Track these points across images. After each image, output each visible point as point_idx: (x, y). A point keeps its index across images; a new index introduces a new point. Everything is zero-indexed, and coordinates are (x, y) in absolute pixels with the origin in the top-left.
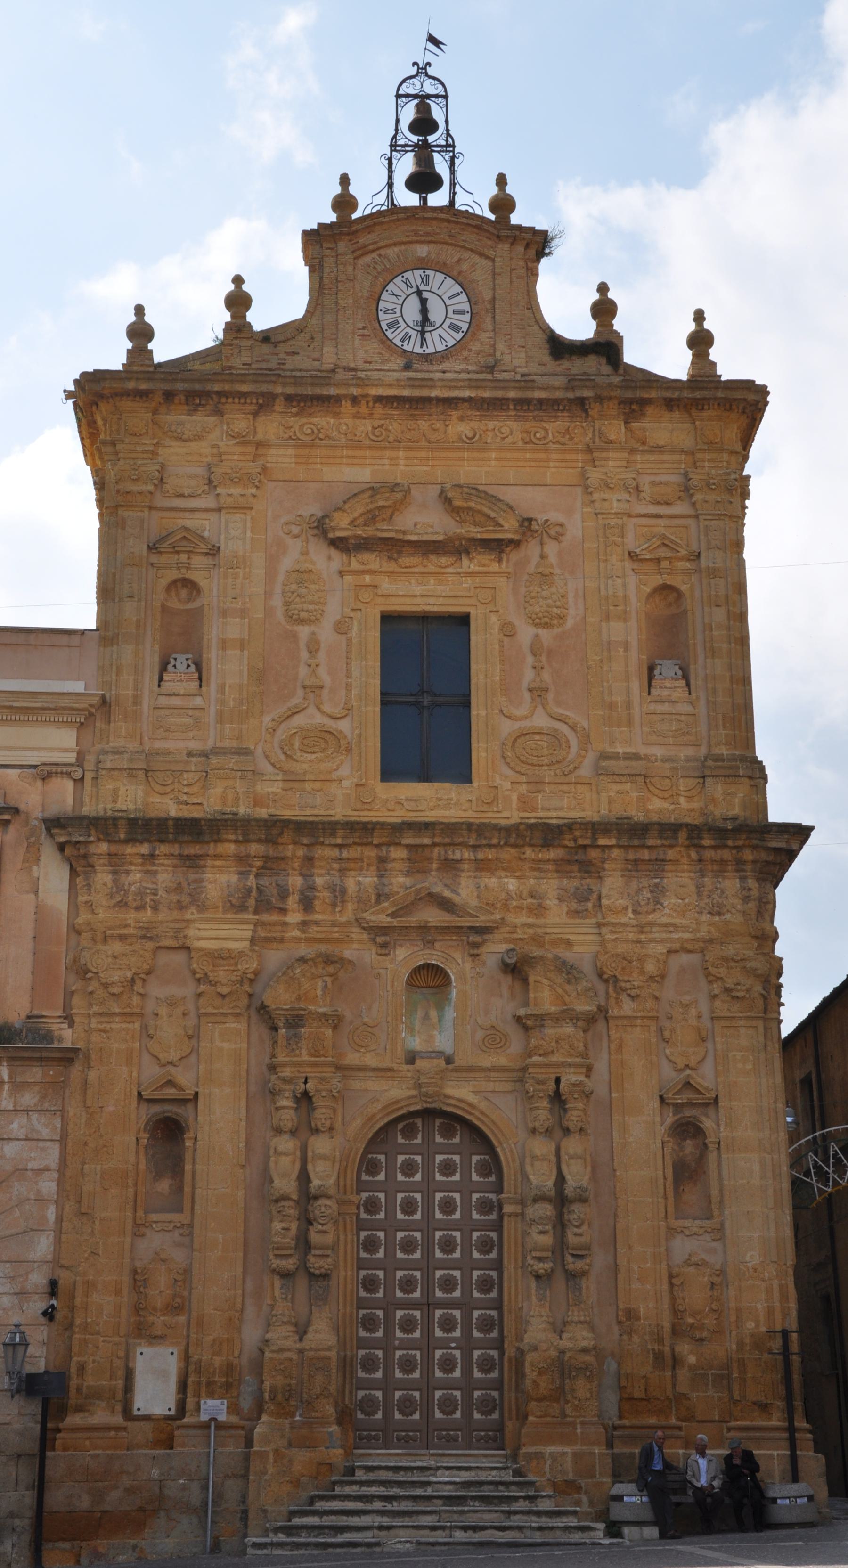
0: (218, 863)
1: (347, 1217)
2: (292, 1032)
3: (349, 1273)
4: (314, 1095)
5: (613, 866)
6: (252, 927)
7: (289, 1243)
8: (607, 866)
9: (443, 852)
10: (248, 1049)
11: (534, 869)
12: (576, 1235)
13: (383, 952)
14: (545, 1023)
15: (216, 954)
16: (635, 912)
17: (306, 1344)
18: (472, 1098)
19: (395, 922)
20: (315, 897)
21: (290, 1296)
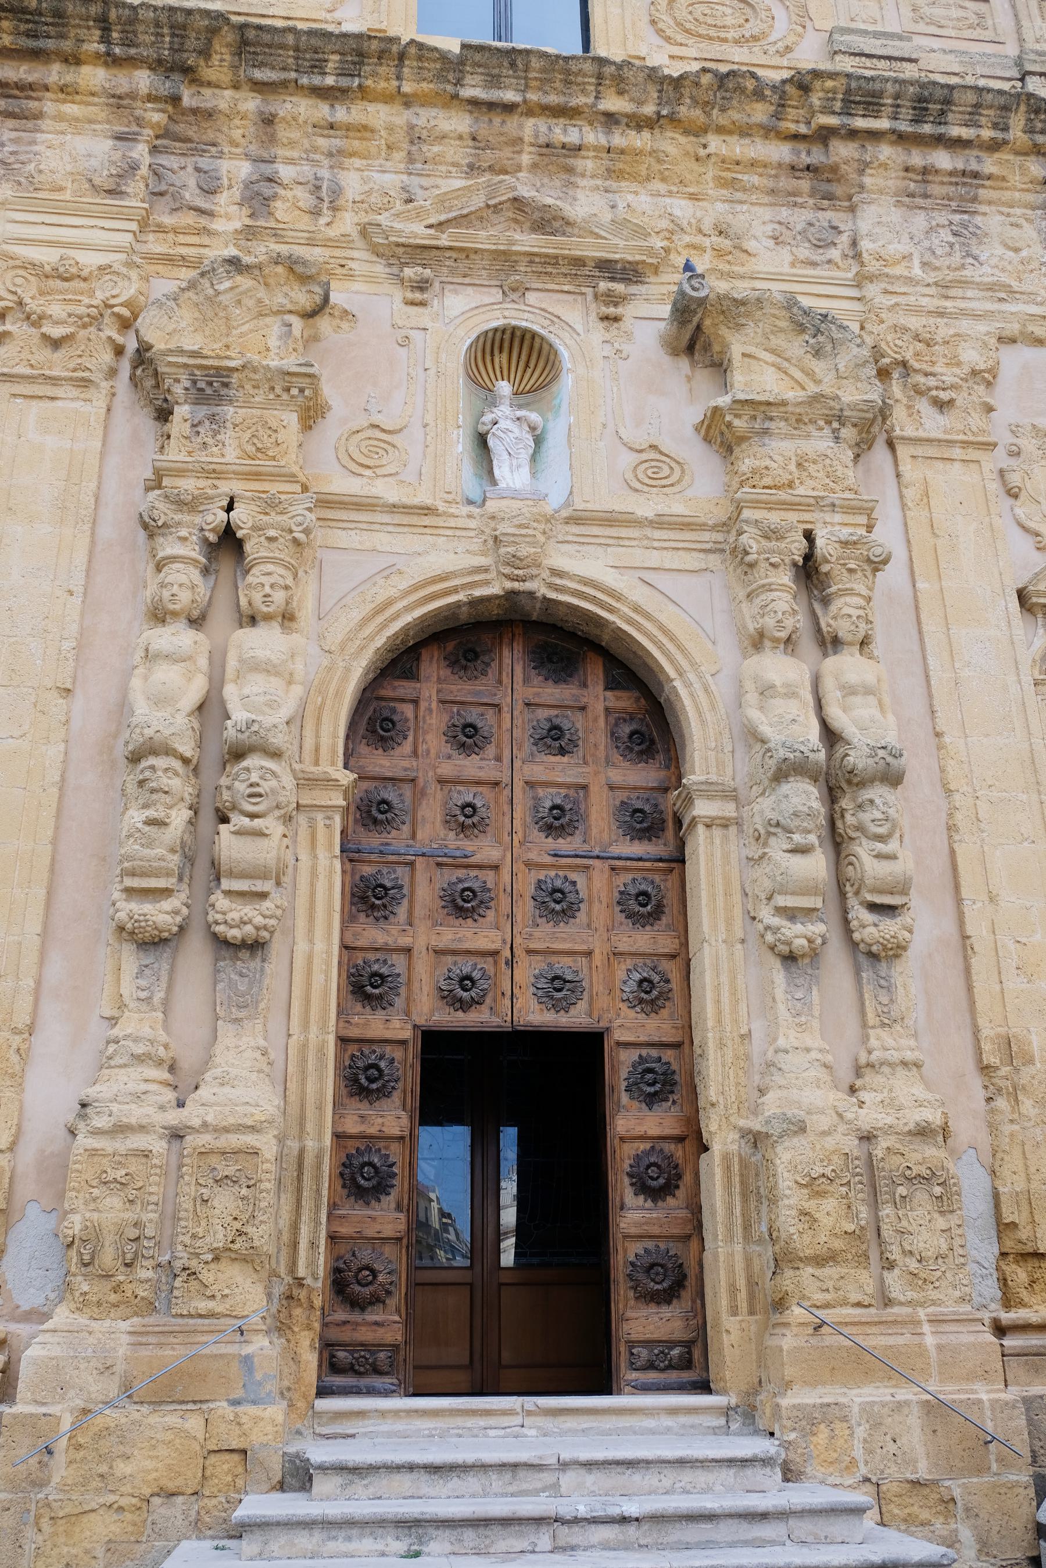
0: (71, 109)
1: (320, 816)
2: (203, 411)
3: (319, 946)
4: (249, 536)
5: (881, 182)
6: (134, 226)
7: (162, 859)
8: (867, 180)
9: (543, 129)
10: (103, 454)
11: (723, 183)
12: (879, 856)
13: (418, 296)
14: (772, 425)
15: (47, 268)
16: (924, 264)
17: (192, 1115)
18: (610, 578)
19: (444, 240)
20: (275, 196)
21: (159, 996)
